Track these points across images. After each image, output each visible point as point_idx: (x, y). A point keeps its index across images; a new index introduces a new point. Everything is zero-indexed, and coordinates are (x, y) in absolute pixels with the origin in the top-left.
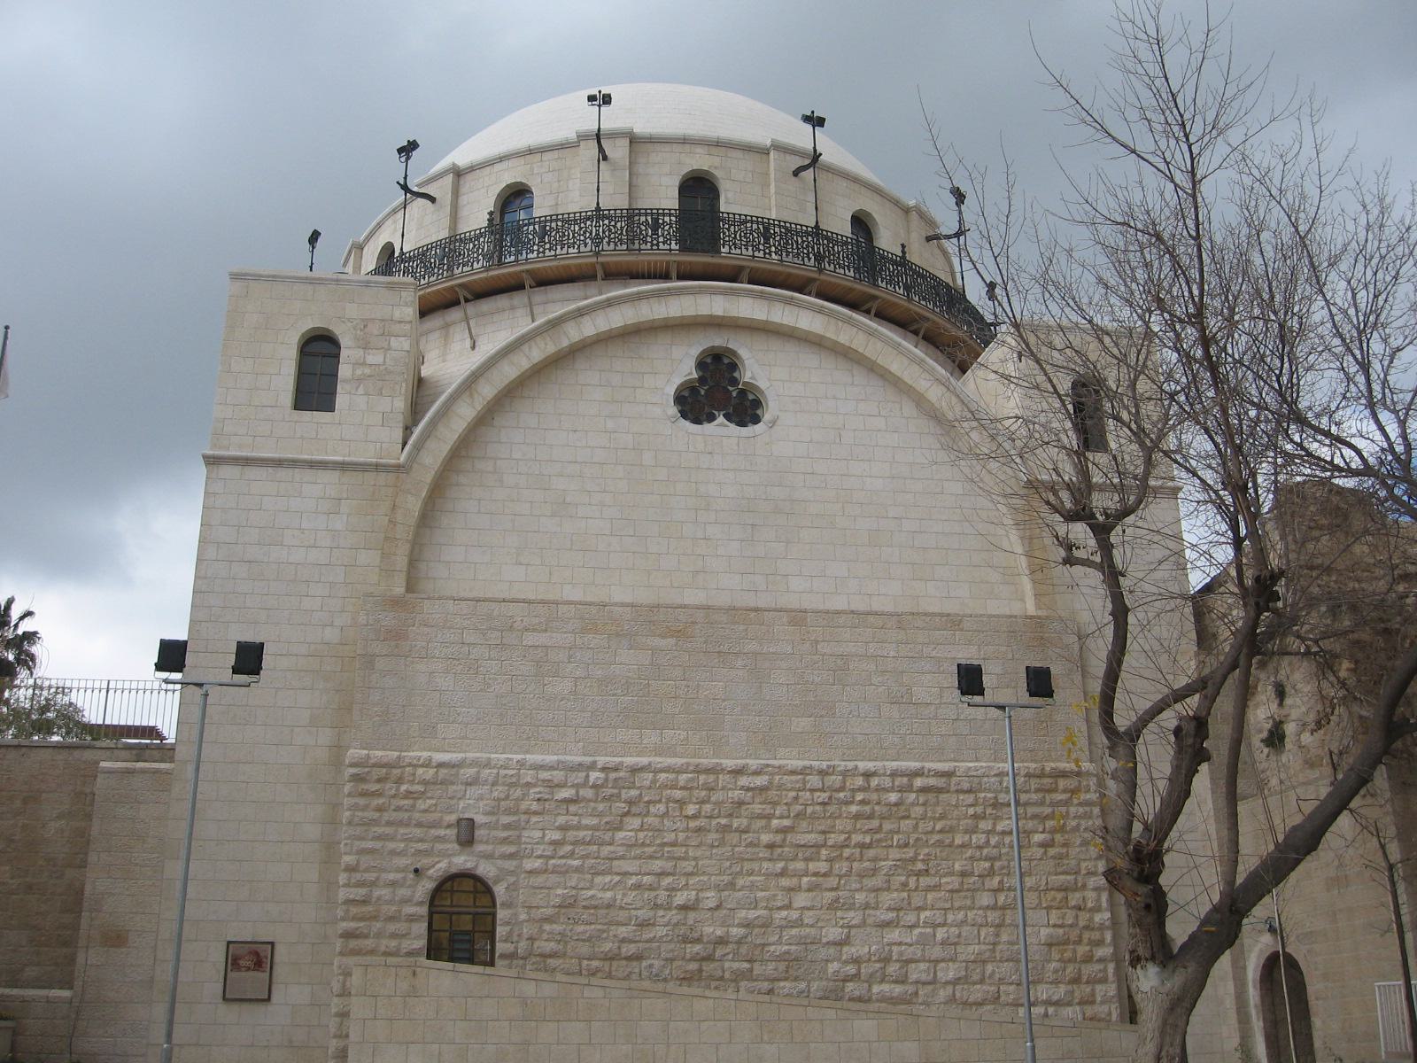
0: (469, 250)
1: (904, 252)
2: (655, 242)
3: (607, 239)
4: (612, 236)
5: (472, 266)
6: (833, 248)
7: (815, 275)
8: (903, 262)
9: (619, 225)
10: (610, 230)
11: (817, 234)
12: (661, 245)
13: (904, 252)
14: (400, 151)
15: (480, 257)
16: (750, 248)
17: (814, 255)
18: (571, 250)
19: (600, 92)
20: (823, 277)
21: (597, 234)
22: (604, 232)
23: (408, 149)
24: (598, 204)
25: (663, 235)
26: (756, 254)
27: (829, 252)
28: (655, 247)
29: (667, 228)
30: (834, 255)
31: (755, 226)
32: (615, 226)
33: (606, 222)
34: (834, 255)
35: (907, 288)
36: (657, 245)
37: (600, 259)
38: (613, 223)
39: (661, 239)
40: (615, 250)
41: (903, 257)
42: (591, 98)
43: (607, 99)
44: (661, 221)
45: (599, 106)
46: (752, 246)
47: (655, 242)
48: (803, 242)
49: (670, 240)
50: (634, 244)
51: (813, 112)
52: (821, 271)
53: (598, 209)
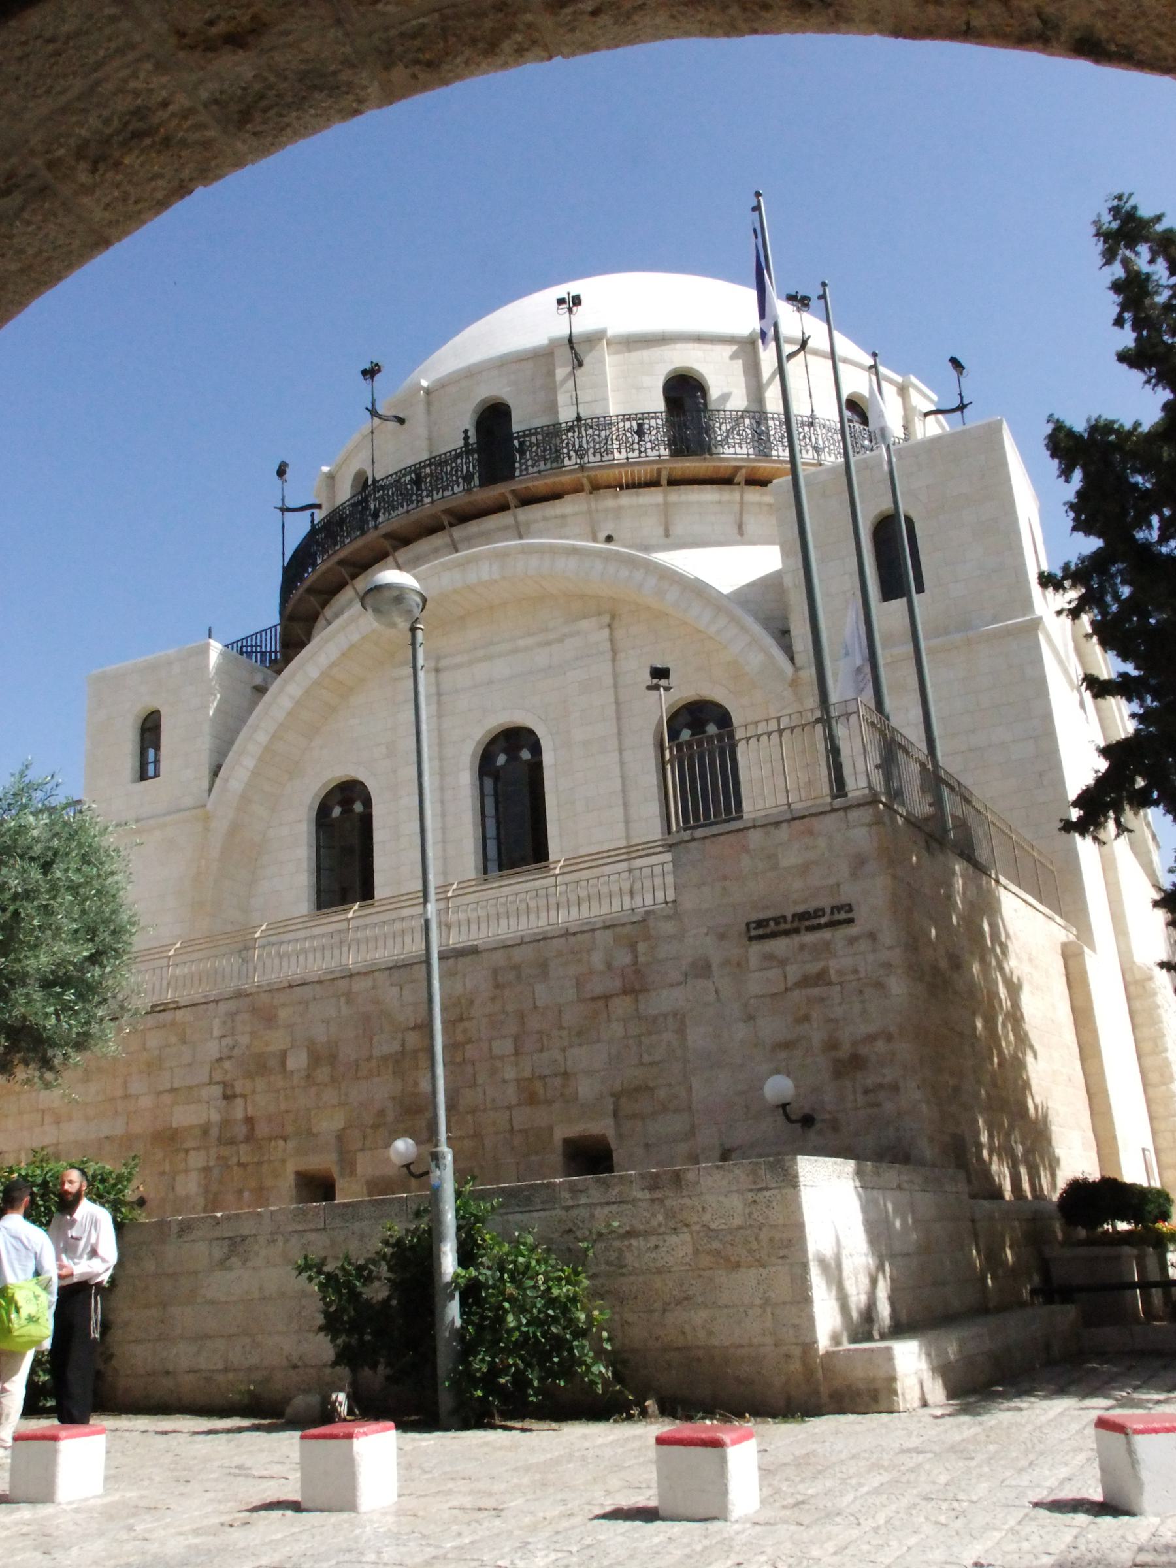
6: (599, 436)
11: (579, 428)
17: (576, 452)
42: (364, 373)
52: (582, 468)
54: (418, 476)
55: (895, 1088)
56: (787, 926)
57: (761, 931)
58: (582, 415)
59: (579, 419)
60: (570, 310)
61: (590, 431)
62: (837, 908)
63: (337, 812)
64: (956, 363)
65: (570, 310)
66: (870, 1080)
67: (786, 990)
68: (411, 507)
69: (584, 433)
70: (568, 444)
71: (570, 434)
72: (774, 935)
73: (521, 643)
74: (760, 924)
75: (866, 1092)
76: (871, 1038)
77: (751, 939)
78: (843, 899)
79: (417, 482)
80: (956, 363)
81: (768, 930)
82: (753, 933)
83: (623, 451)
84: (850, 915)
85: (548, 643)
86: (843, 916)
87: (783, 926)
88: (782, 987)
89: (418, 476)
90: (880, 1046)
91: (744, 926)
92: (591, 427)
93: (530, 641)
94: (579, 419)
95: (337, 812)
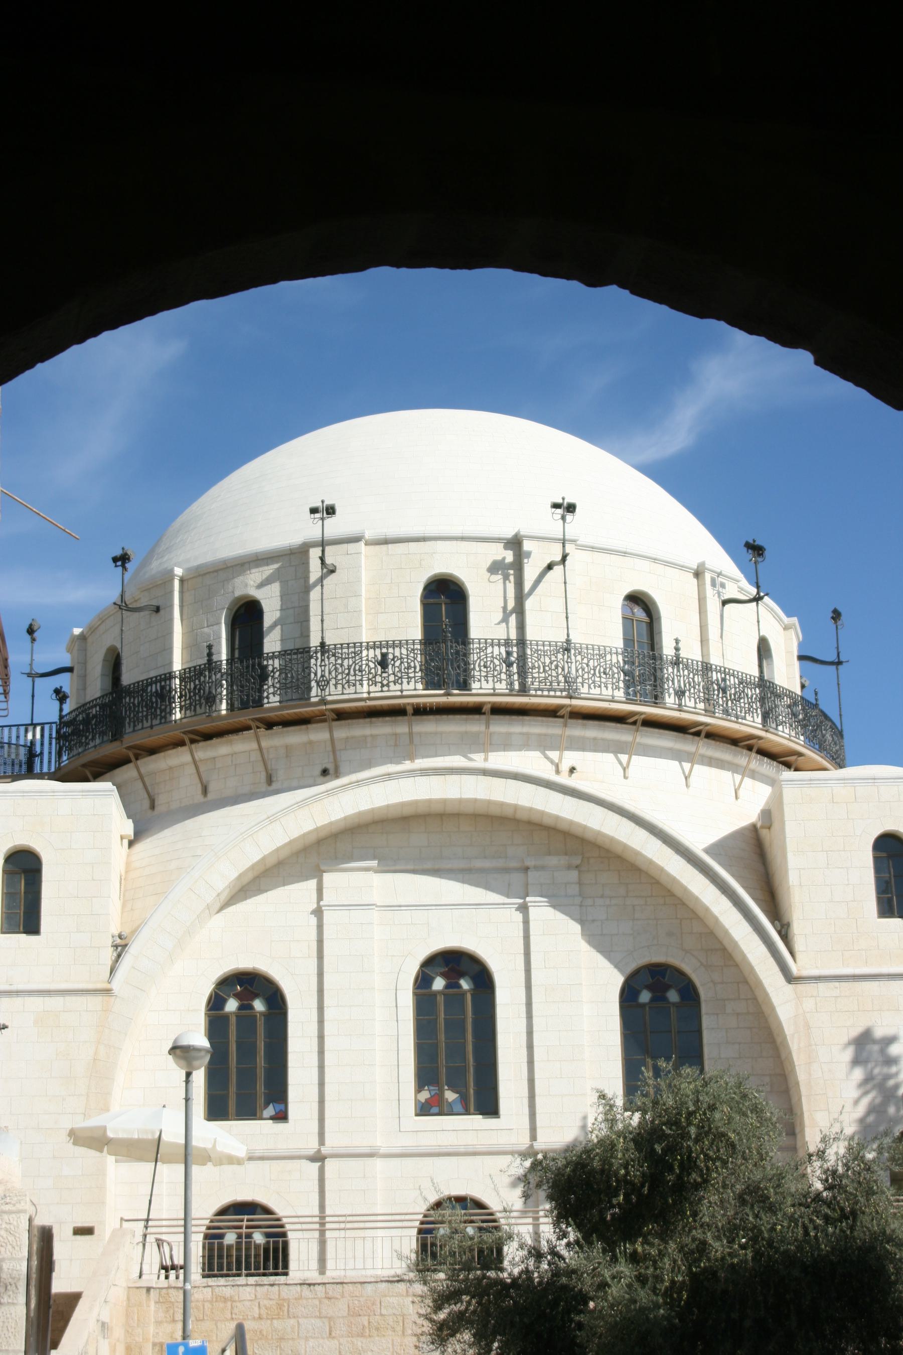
0: (190, 691)
1: (677, 649)
2: (385, 682)
3: (333, 682)
4: (340, 677)
5: (195, 710)
7: (567, 701)
8: (677, 662)
9: (346, 663)
10: (336, 669)
12: (392, 684)
13: (677, 649)
14: (115, 560)
15: (203, 701)
16: (490, 679)
19: (323, 502)
20: (574, 702)
21: (322, 676)
22: (330, 673)
23: (122, 560)
24: (322, 638)
25: (394, 674)
26: (498, 685)
27: (583, 670)
29: (398, 663)
30: (589, 673)
32: (342, 665)
33: (332, 659)
34: (589, 673)
35: (680, 694)
36: (388, 685)
37: (329, 707)
38: (339, 661)
39: (392, 678)
40: (343, 694)
41: (677, 656)
42: (314, 511)
43: (331, 511)
44: (391, 656)
45: (323, 519)
46: (494, 676)
47: (385, 682)
48: (551, 663)
49: (401, 678)
50: (362, 685)
51: (563, 499)
53: (323, 644)
54: (384, 656)
58: (574, 638)
59: (568, 641)
60: (563, 518)
61: (579, 658)
63: (232, 1005)
64: (836, 615)
65: (563, 518)
68: (373, 688)
69: (573, 657)
70: (557, 667)
71: (560, 656)
73: (478, 864)
79: (383, 663)
80: (836, 615)
85: (506, 870)
89: (384, 656)
92: (580, 653)
93: (487, 864)
94: (568, 641)
95: (232, 1005)
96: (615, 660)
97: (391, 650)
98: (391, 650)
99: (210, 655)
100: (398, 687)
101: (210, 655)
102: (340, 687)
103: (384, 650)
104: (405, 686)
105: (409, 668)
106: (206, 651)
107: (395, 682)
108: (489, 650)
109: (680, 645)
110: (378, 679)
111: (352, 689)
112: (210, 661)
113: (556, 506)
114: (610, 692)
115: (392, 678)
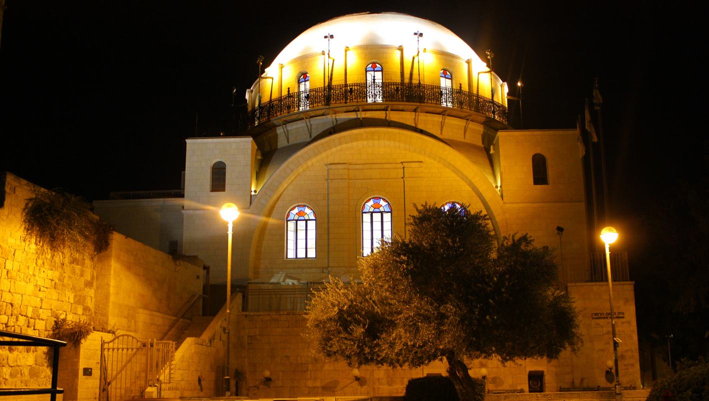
1: (461, 87)
9: (337, 92)
10: (333, 94)
18: (319, 104)
28: (351, 101)
29: (356, 92)
31: (393, 87)
32: (335, 93)
34: (427, 95)
36: (352, 100)
42: (326, 37)
44: (353, 89)
50: (343, 100)
55: (633, 365)
56: (604, 316)
57: (596, 317)
58: (422, 83)
62: (620, 313)
66: (626, 363)
67: (603, 335)
72: (600, 318)
74: (596, 314)
75: (625, 365)
76: (627, 351)
77: (593, 318)
78: (621, 311)
81: (598, 317)
82: (594, 317)
83: (435, 100)
84: (623, 316)
86: (621, 316)
87: (603, 316)
88: (602, 334)
90: (630, 353)
91: (591, 315)
94: (420, 83)
96: (437, 91)
97: (353, 87)
98: (353, 87)
99: (289, 91)
100: (356, 100)
101: (289, 91)
102: (335, 101)
103: (351, 87)
104: (359, 100)
105: (360, 93)
106: (288, 90)
107: (355, 99)
108: (390, 86)
109: (462, 86)
110: (349, 98)
111: (339, 102)
112: (289, 94)
113: (415, 34)
114: (435, 102)
115: (354, 97)
